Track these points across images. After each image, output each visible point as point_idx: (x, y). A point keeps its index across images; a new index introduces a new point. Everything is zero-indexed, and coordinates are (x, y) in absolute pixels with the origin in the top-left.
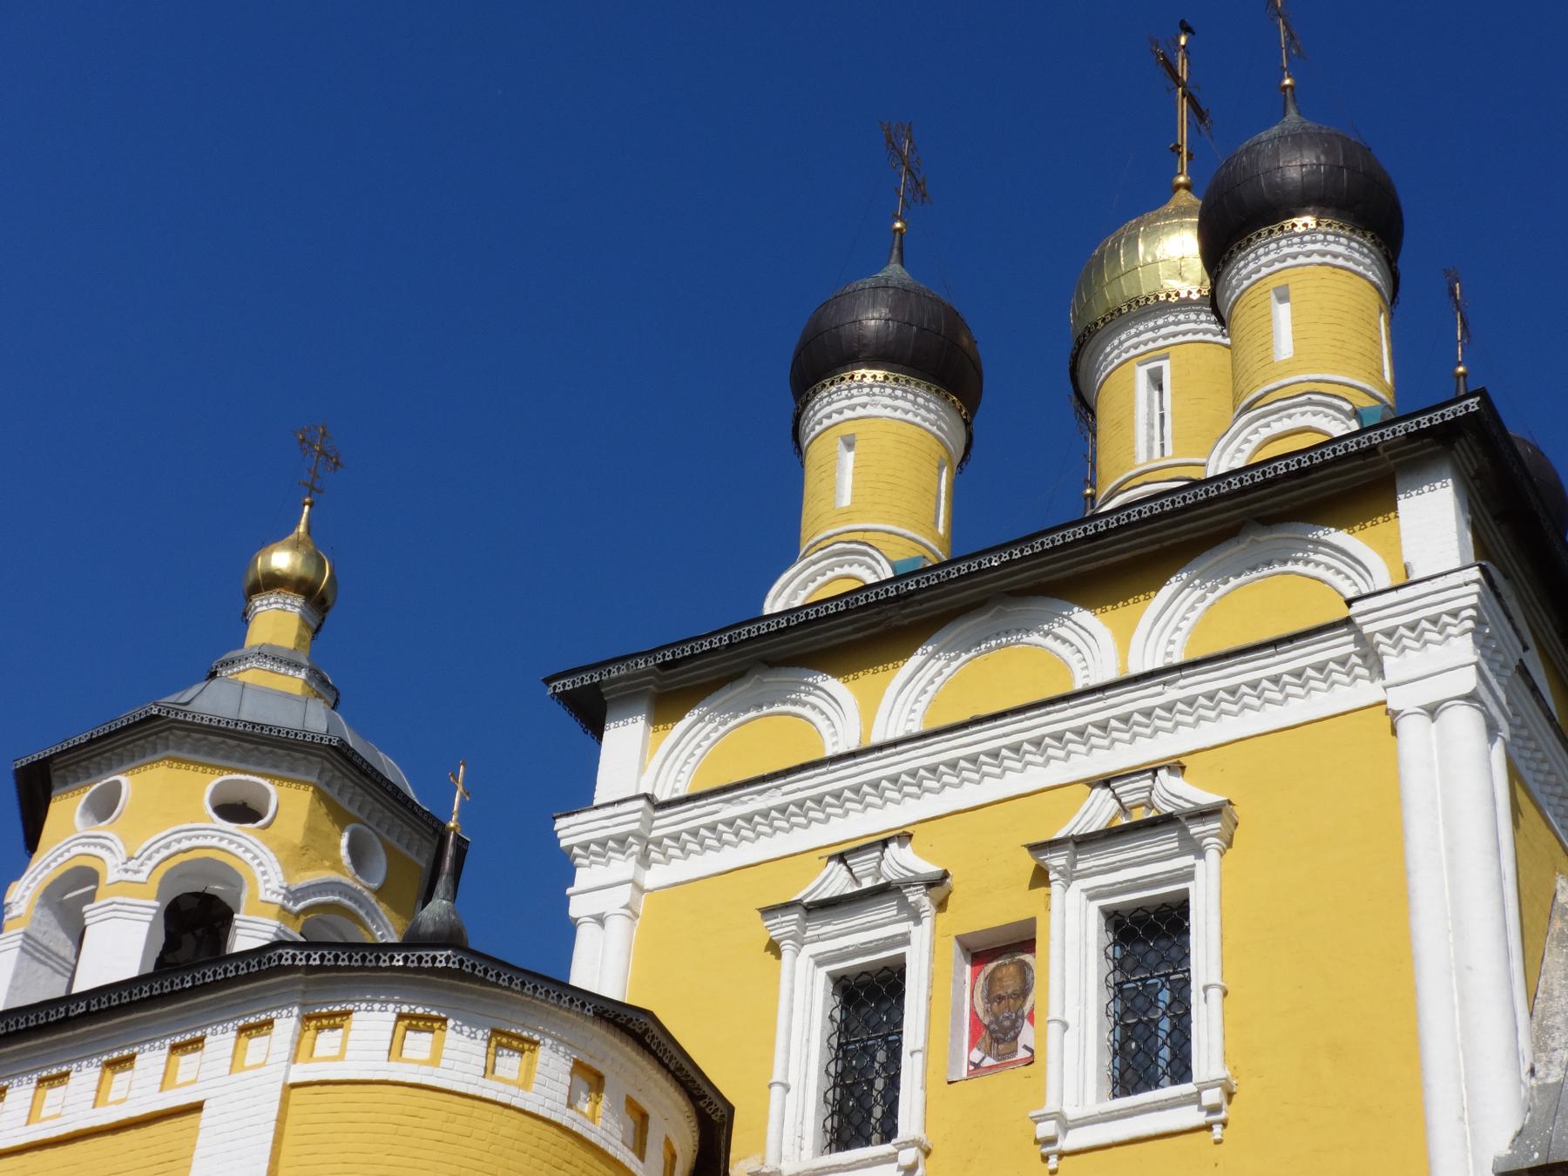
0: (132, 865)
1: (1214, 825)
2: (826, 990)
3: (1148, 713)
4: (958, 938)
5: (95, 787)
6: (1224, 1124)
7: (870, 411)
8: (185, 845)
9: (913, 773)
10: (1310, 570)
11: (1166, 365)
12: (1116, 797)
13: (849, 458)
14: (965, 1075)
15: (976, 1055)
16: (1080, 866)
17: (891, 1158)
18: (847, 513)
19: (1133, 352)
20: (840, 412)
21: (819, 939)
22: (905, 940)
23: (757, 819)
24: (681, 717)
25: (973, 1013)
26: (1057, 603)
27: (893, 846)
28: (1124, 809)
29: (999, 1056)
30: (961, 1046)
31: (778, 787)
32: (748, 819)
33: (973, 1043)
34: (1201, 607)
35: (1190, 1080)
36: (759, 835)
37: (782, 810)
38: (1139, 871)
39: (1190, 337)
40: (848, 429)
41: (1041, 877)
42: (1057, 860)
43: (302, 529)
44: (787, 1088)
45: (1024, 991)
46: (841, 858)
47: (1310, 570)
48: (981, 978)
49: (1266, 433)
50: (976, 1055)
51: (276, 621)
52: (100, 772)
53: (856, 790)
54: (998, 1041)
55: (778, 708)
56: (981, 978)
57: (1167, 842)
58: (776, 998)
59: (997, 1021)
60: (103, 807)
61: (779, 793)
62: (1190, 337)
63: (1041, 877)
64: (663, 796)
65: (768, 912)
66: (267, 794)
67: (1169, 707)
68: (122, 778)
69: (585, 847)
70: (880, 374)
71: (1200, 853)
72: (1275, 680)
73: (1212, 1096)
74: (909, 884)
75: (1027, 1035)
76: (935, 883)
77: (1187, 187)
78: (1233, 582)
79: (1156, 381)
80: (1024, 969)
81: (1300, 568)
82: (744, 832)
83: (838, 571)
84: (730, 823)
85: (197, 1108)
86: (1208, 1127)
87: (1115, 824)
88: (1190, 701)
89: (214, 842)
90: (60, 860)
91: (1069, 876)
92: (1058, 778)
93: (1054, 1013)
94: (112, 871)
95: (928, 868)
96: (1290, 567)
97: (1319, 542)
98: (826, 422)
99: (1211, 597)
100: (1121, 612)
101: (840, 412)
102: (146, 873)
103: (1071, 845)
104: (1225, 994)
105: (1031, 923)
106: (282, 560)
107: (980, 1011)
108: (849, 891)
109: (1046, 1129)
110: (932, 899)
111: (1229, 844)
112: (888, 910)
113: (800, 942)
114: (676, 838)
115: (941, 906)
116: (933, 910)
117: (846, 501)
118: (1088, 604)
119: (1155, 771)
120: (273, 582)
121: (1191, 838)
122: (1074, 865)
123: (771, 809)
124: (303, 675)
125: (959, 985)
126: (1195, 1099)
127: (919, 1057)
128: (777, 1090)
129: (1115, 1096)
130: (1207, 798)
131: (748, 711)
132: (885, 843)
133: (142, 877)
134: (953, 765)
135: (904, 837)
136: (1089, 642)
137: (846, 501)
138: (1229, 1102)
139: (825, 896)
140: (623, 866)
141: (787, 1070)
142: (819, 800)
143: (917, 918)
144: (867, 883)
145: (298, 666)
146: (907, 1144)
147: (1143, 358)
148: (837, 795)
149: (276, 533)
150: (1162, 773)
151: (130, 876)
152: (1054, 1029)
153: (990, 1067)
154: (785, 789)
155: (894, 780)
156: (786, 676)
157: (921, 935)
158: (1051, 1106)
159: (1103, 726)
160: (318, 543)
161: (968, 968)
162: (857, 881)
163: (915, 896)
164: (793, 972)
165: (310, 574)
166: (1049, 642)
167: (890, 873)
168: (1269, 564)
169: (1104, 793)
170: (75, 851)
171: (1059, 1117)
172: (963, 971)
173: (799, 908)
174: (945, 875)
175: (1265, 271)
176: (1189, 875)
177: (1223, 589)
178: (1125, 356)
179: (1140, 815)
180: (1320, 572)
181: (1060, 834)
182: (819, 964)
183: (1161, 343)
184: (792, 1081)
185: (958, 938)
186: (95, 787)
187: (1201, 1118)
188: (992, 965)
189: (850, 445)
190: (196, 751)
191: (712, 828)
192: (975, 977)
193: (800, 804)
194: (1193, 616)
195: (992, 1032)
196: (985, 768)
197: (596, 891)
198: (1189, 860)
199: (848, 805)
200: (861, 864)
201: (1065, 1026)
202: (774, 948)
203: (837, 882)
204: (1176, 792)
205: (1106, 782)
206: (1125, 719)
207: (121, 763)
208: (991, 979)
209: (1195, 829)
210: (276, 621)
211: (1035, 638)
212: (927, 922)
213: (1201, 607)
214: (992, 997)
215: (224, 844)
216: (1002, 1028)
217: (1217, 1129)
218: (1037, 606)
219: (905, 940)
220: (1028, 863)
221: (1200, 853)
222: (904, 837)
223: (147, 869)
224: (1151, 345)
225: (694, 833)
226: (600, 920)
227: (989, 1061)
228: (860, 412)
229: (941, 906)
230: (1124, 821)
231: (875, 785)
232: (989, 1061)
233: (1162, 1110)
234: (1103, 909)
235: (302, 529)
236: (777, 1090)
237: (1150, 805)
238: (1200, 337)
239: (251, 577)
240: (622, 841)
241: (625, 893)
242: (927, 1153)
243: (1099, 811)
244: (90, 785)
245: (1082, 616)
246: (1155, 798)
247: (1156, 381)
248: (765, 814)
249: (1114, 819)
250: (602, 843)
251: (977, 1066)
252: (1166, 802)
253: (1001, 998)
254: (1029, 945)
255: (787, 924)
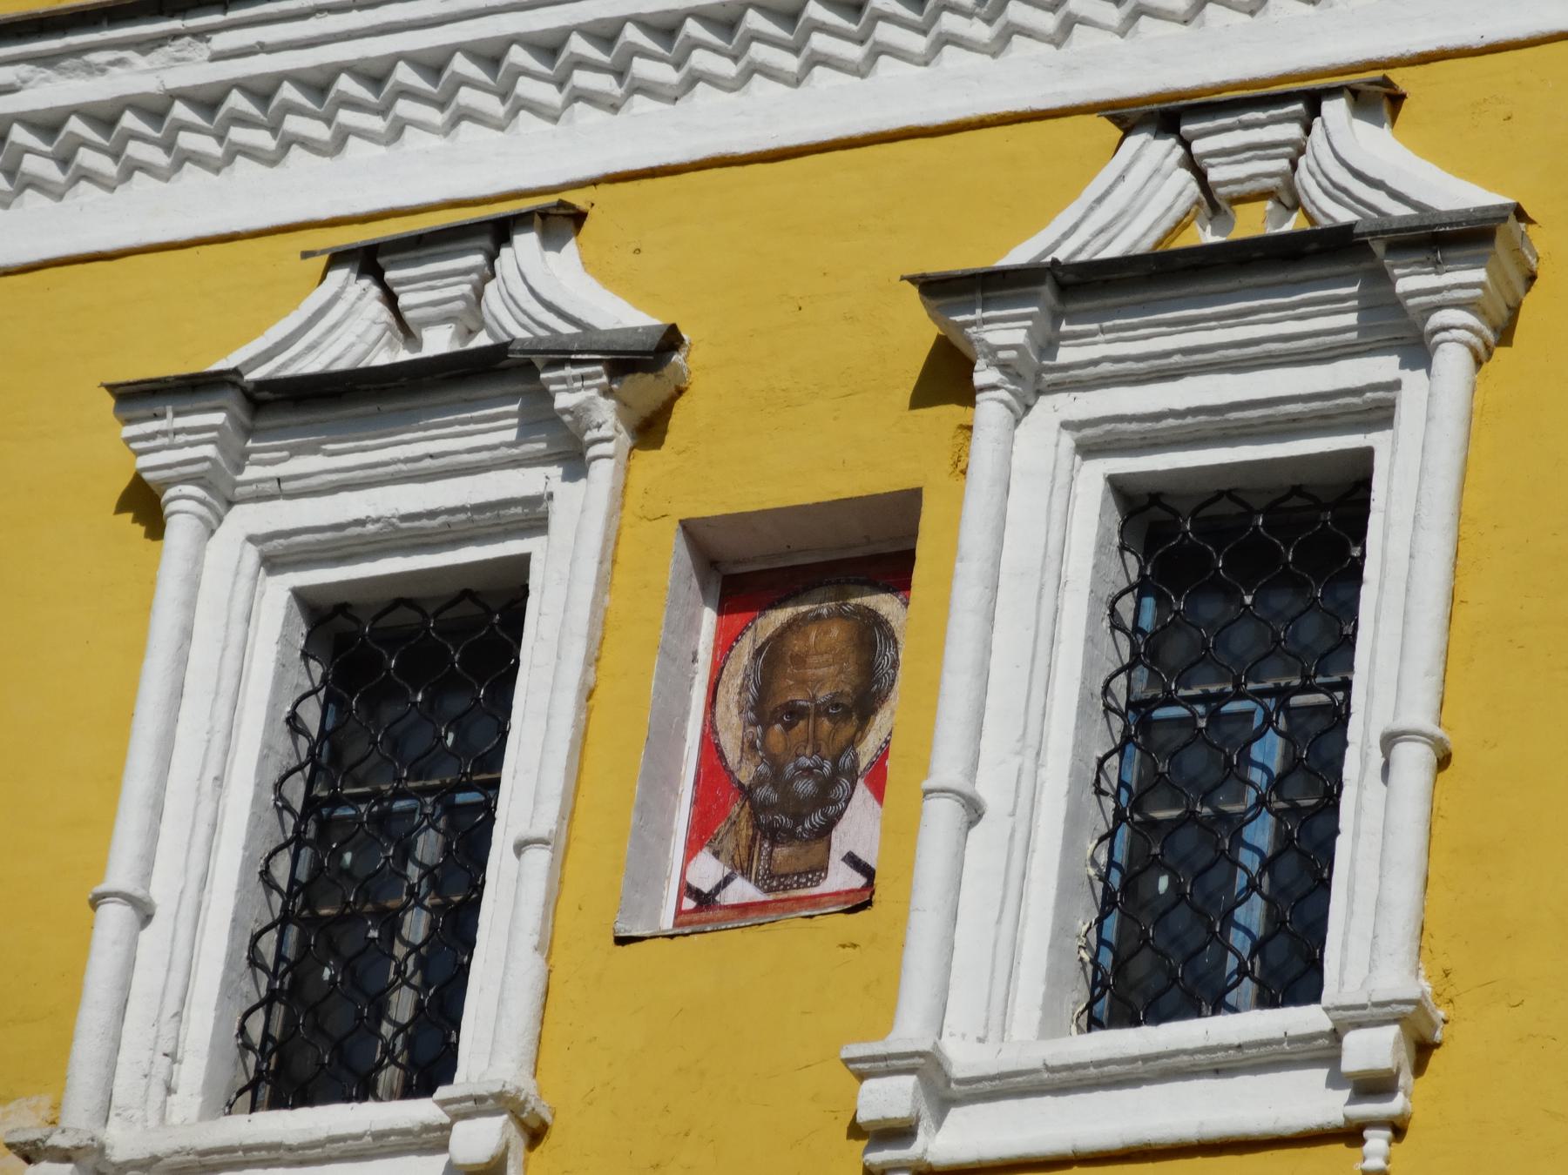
2: (285, 640)
4: (691, 530)
6: (1398, 1129)
12: (1193, 165)
14: (667, 922)
15: (707, 871)
16: (1066, 355)
17: (432, 1140)
21: (280, 491)
22: (531, 517)
23: (129, 121)
25: (710, 747)
27: (526, 243)
28: (1212, 202)
29: (772, 879)
30: (665, 836)
31: (201, 35)
32: (104, 118)
33: (700, 836)
35: (1315, 997)
36: (131, 168)
37: (208, 102)
38: (1233, 385)
41: (947, 377)
42: (1003, 331)
44: (144, 913)
45: (865, 700)
46: (368, 261)
48: (745, 649)
50: (707, 871)
53: (433, 65)
54: (774, 835)
56: (745, 649)
57: (1331, 311)
58: (136, 651)
59: (776, 776)
61: (201, 50)
63: (947, 377)
65: (136, 397)
71: (1418, 351)
73: (1372, 1049)
74: (560, 356)
75: (860, 826)
76: (643, 361)
80: (873, 637)
82: (86, 158)
86: (1352, 1134)
87: (1183, 241)
91: (1033, 380)
93: (946, 769)
95: (618, 314)
103: (1047, 291)
104: (1444, 762)
105: (908, 503)
107: (730, 743)
108: (382, 358)
109: (887, 1098)
110: (624, 405)
111: (1505, 334)
112: (494, 427)
113: (223, 495)
115: (649, 430)
116: (625, 439)
119: (1313, 101)
121: (1396, 304)
122: (1048, 347)
123: (174, 95)
125: (677, 659)
126: (1322, 1052)
127: (539, 858)
128: (114, 916)
129: (1094, 1023)
130: (1453, 194)
132: (500, 232)
135: (558, 219)
138: (1419, 1068)
139: (312, 365)
141: (148, 861)
142: (318, 85)
143: (574, 461)
144: (438, 342)
146: (480, 1105)
148: (375, 76)
150: (1335, 110)
152: (941, 815)
153: (744, 908)
154: (221, 41)
157: (581, 509)
158: (909, 1033)
161: (709, 618)
162: (406, 330)
164: (193, 582)
167: (508, 318)
169: (1155, 151)
171: (926, 1067)
172: (693, 625)
173: (230, 398)
174: (671, 339)
176: (1378, 411)
179: (1253, 222)
181: (1020, 255)
182: (272, 564)
184: (161, 892)
185: (691, 530)
187: (1333, 1107)
188: (779, 617)
192: (725, 645)
193: (262, 91)
195: (757, 809)
196: (819, 41)
198: (1383, 367)
199: (404, 107)
200: (428, 287)
201: (974, 810)
202: (144, 504)
203: (348, 330)
205: (1166, 116)
208: (772, 655)
209: (1410, 281)
212: (602, 473)
214: (767, 708)
216: (789, 799)
217: (1377, 1141)
219: (531, 517)
220: (918, 329)
221: (1418, 351)
222: (558, 219)
227: (742, 891)
229: (649, 430)
230: (1208, 237)
232: (742, 891)
233: (1227, 1078)
234: (1119, 487)
236: (114, 916)
237: (1288, 197)
242: (535, 1135)
243: (1138, 199)
246: (1304, 178)
248: (154, 110)
249: (1180, 226)
251: (705, 900)
252: (1337, 192)
253: (794, 713)
254: (893, 568)
255: (189, 438)
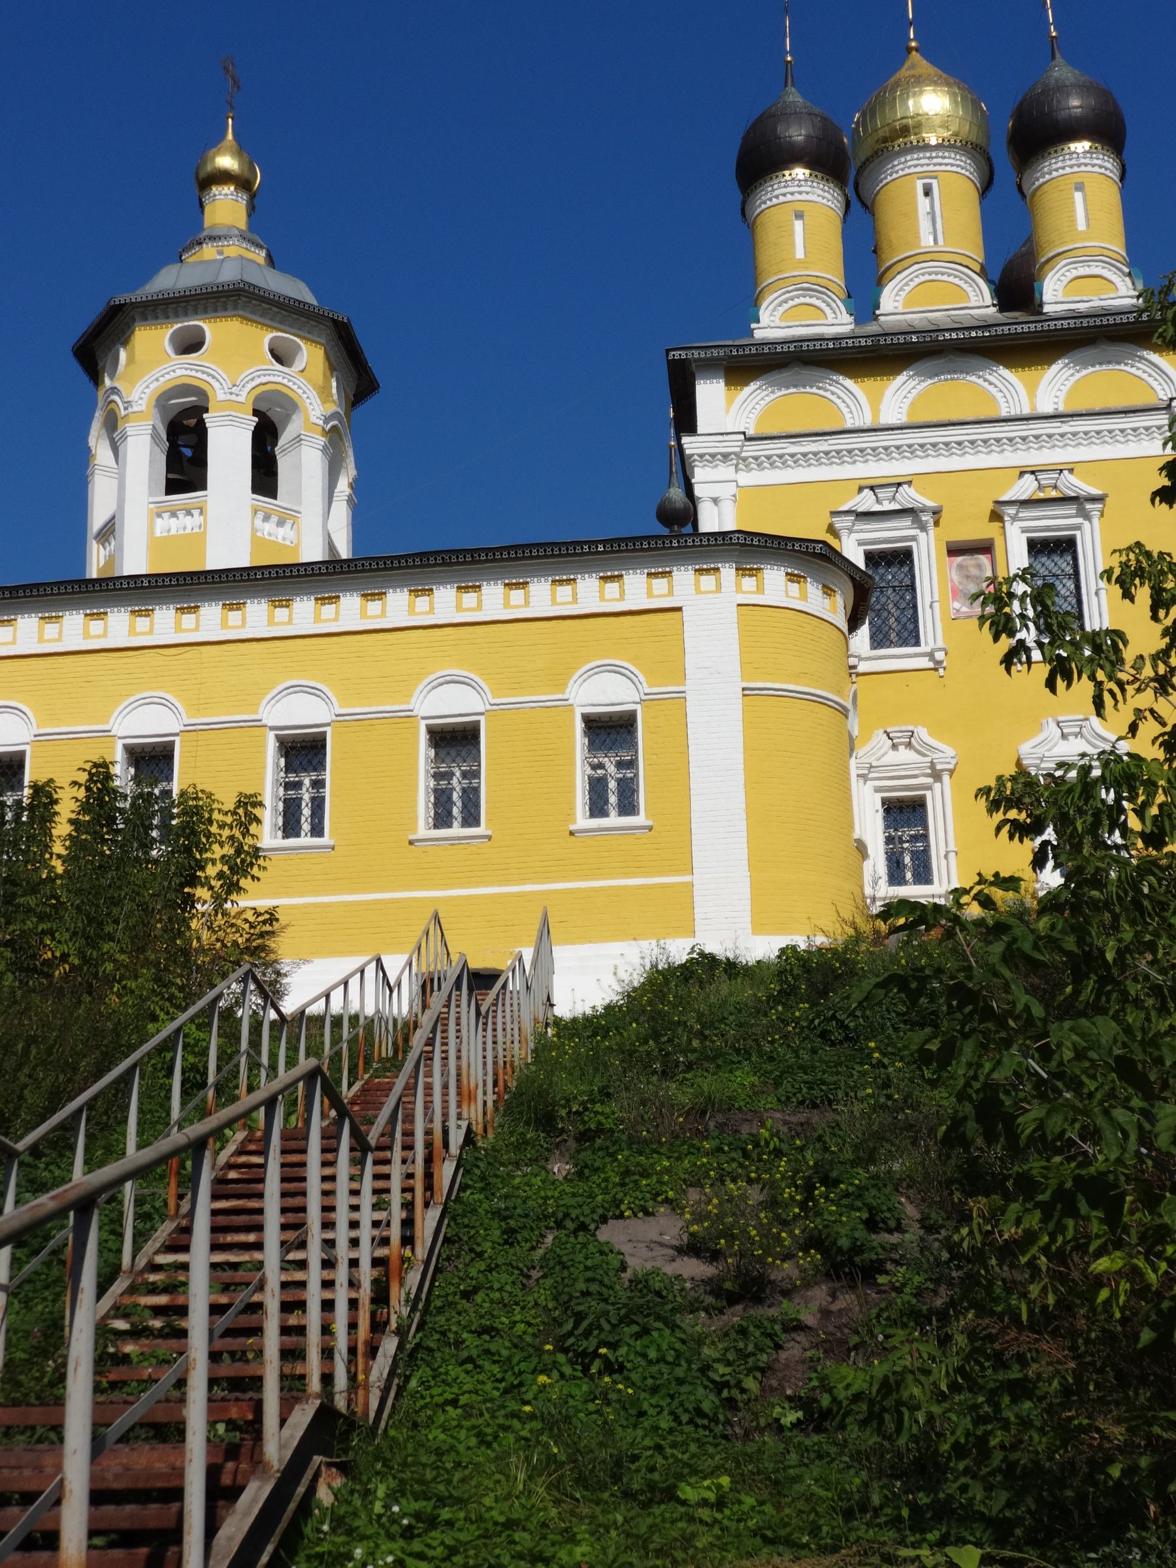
0: (234, 390)
1: (1099, 506)
3: (1050, 436)
5: (176, 326)
7: (810, 197)
8: (267, 379)
9: (910, 446)
10: (1133, 370)
11: (934, 182)
13: (798, 225)
15: (957, 605)
18: (800, 261)
19: (913, 170)
20: (792, 194)
21: (861, 531)
24: (747, 384)
26: (987, 361)
28: (1041, 488)
32: (804, 455)
34: (1073, 379)
37: (827, 453)
38: (1053, 522)
39: (948, 168)
40: (799, 207)
41: (996, 517)
42: (1011, 511)
43: (230, 136)
46: (872, 488)
47: (1133, 370)
49: (1075, 273)
51: (226, 207)
52: (186, 314)
53: (874, 449)
55: (808, 389)
57: (1071, 510)
60: (190, 344)
62: (948, 168)
64: (751, 432)
65: (834, 513)
66: (299, 348)
67: (1062, 435)
68: (206, 326)
69: (701, 456)
70: (807, 172)
72: (1122, 431)
76: (936, 512)
77: (917, 50)
78: (1091, 369)
79: (927, 192)
81: (1128, 368)
83: (802, 300)
84: (792, 455)
85: (679, 609)
88: (1074, 434)
89: (279, 379)
90: (168, 377)
91: (1014, 519)
92: (1002, 464)
94: (219, 393)
96: (1122, 367)
97: (1142, 358)
98: (782, 199)
99: (1078, 376)
100: (1030, 373)
101: (792, 194)
102: (244, 396)
106: (226, 161)
112: (907, 522)
113: (851, 531)
114: (756, 458)
115: (936, 524)
117: (800, 254)
118: (1007, 366)
120: (224, 177)
124: (263, 254)
131: (788, 388)
132: (899, 484)
133: (242, 399)
134: (934, 445)
136: (1006, 388)
137: (800, 254)
140: (725, 471)
142: (850, 451)
143: (923, 528)
145: (261, 247)
147: (921, 175)
148: (862, 450)
149: (215, 140)
151: (233, 397)
155: (898, 448)
156: (816, 372)
159: (1024, 439)
160: (242, 148)
163: (926, 518)
165: (247, 174)
166: (980, 381)
168: (1109, 362)
169: (1029, 478)
170: (179, 372)
175: (1068, 170)
177: (1085, 372)
178: (907, 171)
180: (1139, 373)
183: (931, 168)
186: (176, 326)
189: (799, 216)
190: (253, 312)
191: (780, 456)
193: (838, 452)
194: (1069, 384)
197: (707, 481)
198: (1080, 520)
200: (882, 494)
203: (867, 502)
204: (1074, 484)
205: (1033, 472)
206: (1037, 437)
207: (205, 311)
209: (1088, 506)
210: (226, 207)
211: (973, 378)
213: (1073, 379)
215: (285, 381)
218: (974, 361)
223: (244, 393)
224: (926, 168)
225: (768, 457)
226: (715, 501)
227: (964, 609)
228: (804, 197)
229: (936, 524)
230: (1041, 495)
231: (886, 448)
235: (230, 136)
237: (1055, 487)
238: (954, 169)
239: (209, 168)
240: (726, 456)
241: (731, 489)
243: (1026, 488)
244: (172, 324)
245: (1003, 371)
247: (927, 192)
248: (815, 454)
250: (713, 456)
